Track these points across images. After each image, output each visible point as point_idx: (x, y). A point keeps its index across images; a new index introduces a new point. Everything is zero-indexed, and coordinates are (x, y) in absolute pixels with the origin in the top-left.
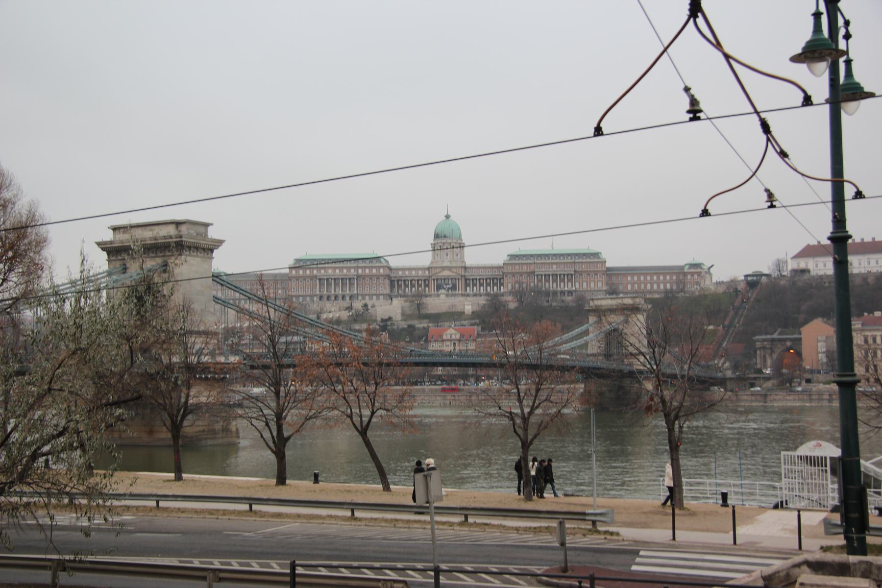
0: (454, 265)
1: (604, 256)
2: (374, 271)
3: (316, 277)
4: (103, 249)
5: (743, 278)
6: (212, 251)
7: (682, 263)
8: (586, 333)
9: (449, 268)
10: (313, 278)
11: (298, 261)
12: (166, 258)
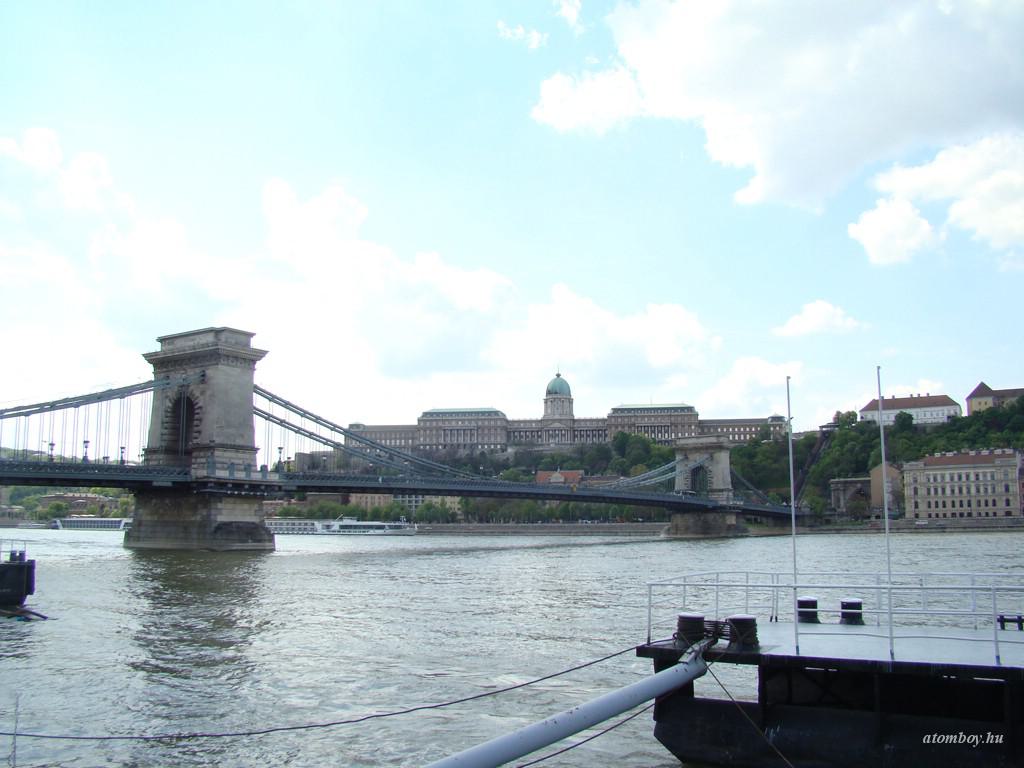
0: (563, 418)
1: (697, 409)
2: (492, 423)
3: (441, 427)
4: (150, 362)
5: (818, 429)
6: (254, 362)
7: (766, 417)
8: (673, 469)
9: (560, 421)
10: (438, 429)
11: (425, 414)
12: (203, 368)
